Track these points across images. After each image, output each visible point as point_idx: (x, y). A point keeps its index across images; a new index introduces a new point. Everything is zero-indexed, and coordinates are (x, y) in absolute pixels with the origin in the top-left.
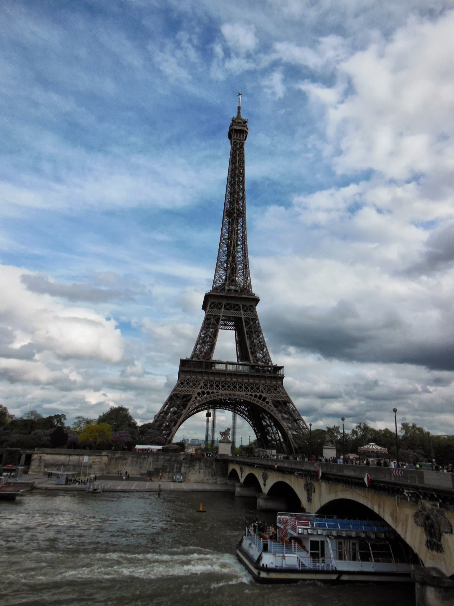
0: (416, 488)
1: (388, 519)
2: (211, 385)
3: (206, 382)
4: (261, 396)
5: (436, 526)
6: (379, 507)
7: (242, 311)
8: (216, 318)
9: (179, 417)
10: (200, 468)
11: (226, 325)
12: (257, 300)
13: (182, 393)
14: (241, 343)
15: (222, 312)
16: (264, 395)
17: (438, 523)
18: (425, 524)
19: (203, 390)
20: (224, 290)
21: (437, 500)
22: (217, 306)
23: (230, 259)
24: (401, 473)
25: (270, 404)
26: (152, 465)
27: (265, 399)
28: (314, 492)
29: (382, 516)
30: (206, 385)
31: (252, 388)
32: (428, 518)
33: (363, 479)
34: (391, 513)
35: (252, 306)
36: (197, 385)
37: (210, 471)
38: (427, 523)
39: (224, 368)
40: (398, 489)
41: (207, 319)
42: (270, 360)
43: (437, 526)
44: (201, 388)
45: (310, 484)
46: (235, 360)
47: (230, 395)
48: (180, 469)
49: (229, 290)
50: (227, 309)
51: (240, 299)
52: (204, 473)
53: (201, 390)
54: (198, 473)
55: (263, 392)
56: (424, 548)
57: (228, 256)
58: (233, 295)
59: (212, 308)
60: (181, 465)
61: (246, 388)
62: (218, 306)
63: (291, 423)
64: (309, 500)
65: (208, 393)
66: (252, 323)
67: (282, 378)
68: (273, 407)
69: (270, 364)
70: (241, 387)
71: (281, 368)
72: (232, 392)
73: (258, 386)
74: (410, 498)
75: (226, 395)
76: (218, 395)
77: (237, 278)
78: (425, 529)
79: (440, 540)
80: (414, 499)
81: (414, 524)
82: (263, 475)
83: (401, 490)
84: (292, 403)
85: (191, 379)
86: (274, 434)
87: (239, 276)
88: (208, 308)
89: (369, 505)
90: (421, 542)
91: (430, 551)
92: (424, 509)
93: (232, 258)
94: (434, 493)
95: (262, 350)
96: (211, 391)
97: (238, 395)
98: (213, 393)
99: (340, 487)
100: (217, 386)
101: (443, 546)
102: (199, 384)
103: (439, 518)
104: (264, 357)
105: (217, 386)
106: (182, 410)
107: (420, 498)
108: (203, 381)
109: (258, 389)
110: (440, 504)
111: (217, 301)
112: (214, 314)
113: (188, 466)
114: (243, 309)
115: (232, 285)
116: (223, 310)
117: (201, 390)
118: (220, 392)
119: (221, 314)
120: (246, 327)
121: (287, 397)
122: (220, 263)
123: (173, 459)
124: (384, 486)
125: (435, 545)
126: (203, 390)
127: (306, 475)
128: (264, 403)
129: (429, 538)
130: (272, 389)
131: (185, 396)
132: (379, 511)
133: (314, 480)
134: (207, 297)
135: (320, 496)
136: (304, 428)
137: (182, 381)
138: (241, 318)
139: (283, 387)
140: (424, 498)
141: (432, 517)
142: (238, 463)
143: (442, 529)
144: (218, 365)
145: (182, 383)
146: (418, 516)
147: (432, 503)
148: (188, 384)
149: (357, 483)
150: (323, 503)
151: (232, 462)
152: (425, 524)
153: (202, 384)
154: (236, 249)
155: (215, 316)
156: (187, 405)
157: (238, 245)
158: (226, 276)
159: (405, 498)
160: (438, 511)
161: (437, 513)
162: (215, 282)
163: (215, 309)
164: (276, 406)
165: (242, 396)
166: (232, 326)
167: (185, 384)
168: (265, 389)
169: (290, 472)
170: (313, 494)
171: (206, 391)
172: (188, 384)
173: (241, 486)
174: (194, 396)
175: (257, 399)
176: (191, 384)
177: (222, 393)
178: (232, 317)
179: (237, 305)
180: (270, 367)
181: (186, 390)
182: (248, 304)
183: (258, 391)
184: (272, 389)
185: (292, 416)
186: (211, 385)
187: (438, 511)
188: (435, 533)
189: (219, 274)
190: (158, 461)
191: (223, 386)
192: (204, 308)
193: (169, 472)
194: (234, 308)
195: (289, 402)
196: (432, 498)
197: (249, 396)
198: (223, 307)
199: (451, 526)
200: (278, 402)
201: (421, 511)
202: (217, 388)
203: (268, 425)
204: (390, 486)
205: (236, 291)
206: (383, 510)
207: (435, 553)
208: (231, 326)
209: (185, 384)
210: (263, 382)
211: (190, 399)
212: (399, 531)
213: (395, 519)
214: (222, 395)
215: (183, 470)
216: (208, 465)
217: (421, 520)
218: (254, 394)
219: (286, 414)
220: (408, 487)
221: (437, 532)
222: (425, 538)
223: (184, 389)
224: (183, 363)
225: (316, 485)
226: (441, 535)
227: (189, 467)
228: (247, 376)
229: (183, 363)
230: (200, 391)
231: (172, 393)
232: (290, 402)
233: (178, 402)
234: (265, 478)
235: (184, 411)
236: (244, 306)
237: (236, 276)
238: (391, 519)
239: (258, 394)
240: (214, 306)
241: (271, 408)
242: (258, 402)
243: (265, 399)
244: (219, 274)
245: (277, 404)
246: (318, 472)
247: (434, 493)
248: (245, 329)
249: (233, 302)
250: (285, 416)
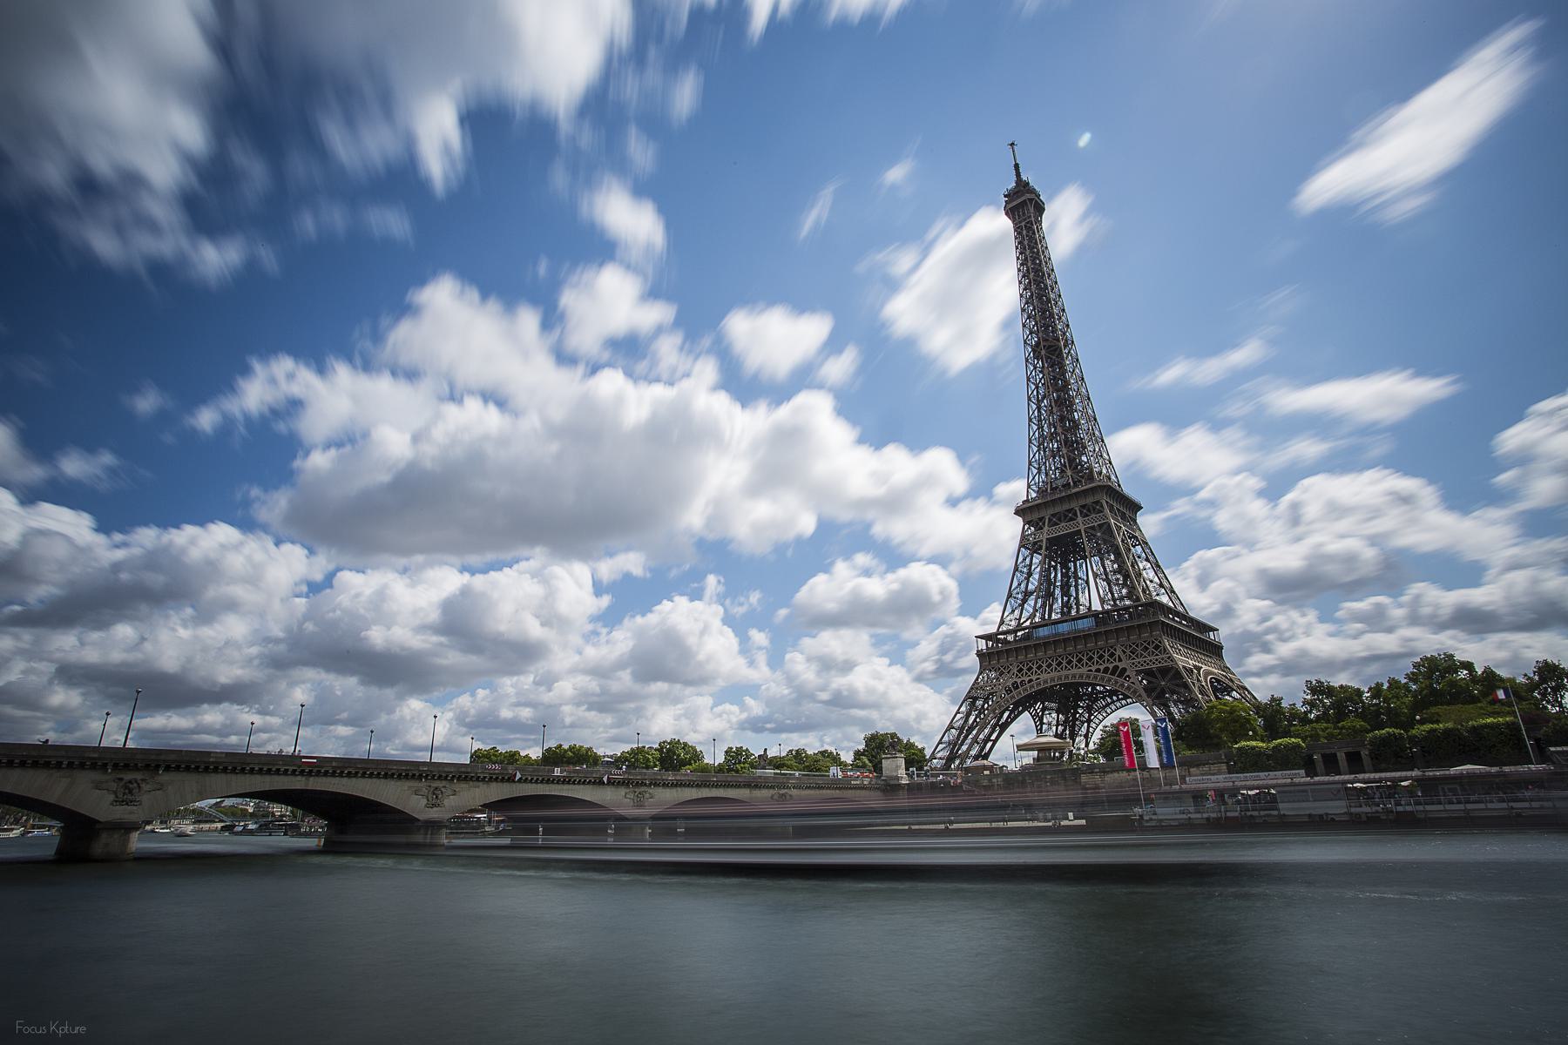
7: (1080, 519)
27: (1124, 670)
31: (1101, 657)
35: (1097, 503)
61: (1090, 659)
97: (1074, 676)
109: (1112, 655)
111: (1036, 516)
118: (1044, 676)
179: (1069, 511)
182: (1089, 500)
236: (1083, 507)
243: (1124, 670)
249: (1066, 507)
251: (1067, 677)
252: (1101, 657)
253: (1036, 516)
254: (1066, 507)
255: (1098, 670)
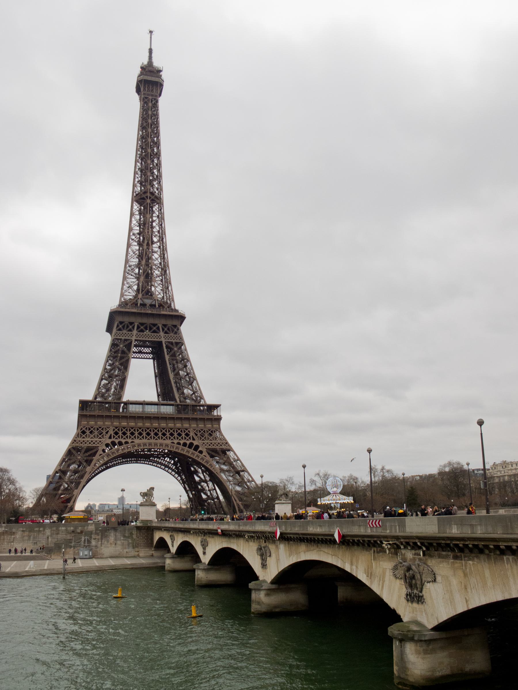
0: (397, 538)
1: (362, 577)
2: (124, 434)
3: (116, 430)
4: (191, 445)
5: (418, 576)
6: (352, 564)
7: (162, 334)
8: (127, 343)
9: (82, 477)
10: (116, 539)
11: (140, 352)
12: (181, 318)
13: (85, 446)
14: (162, 375)
15: (134, 336)
16: (195, 443)
17: (420, 573)
18: (405, 576)
19: (113, 440)
20: (137, 304)
21: (420, 548)
22: (128, 327)
23: (144, 262)
24: (379, 523)
25: (204, 454)
26: (50, 539)
27: (197, 447)
28: (270, 556)
29: (354, 574)
30: (116, 433)
31: (179, 435)
32: (409, 569)
33: (333, 535)
34: (365, 570)
35: (175, 326)
36: (104, 432)
37: (130, 541)
38: (407, 574)
39: (141, 410)
40: (375, 542)
41: (114, 345)
42: (202, 398)
43: (419, 577)
44: (110, 438)
45: (264, 547)
46: (154, 398)
47: (150, 444)
48: (89, 542)
49: (143, 305)
50: (142, 331)
51: (159, 316)
52: (123, 544)
53: (111, 440)
54: (114, 545)
55: (194, 439)
56: (403, 601)
57: (140, 257)
58: (150, 312)
59: (120, 330)
60: (91, 537)
61: (172, 434)
62: (128, 327)
63: (232, 476)
64: (264, 566)
65: (120, 444)
66: (176, 349)
67: (218, 419)
68: (208, 458)
69: (202, 402)
70: (164, 434)
71: (216, 407)
72: (153, 441)
73: (187, 431)
74: (389, 549)
75: (145, 444)
76: (134, 446)
77: (153, 289)
78: (406, 581)
79: (421, 592)
80: (393, 550)
81: (392, 578)
82: (201, 542)
83: (379, 542)
84: (233, 451)
85: (96, 427)
86: (209, 490)
87: (156, 285)
88: (114, 330)
89: (339, 565)
90: (399, 597)
91: (410, 604)
92: (405, 560)
93: (146, 261)
94: (417, 541)
95: (191, 384)
96: (123, 441)
97: (161, 445)
98: (126, 443)
99: (303, 547)
100: (132, 434)
101: (424, 597)
102: (107, 433)
103: (421, 568)
104: (194, 393)
105: (132, 434)
106: (85, 467)
107: (400, 548)
108: (112, 428)
109: (187, 435)
110: (424, 552)
111: (127, 320)
112: (123, 338)
113: (100, 537)
114: (163, 330)
115: (147, 298)
116: (135, 332)
117: (111, 440)
118: (137, 441)
119: (134, 338)
120: (168, 354)
121: (226, 443)
122: (128, 268)
123: (79, 531)
124: (358, 541)
125: (415, 597)
126: (113, 440)
127: (258, 538)
128: (197, 453)
129: (409, 590)
130: (206, 435)
131: (88, 449)
132: (351, 569)
133: (269, 542)
134: (113, 315)
135: (278, 560)
136: (249, 481)
137: (84, 429)
138: (161, 342)
139: (220, 432)
140: (405, 547)
141: (413, 567)
142: (167, 529)
143: (424, 579)
144: (131, 406)
145: (84, 432)
146: (397, 569)
147: (413, 552)
148: (91, 432)
149: (326, 541)
150: (281, 568)
151: (159, 529)
152: (405, 576)
153: (111, 432)
154: (150, 248)
155: (126, 340)
156: (91, 461)
157: (153, 242)
158: (138, 285)
159: (383, 551)
160: (420, 560)
161: (419, 563)
162: (122, 295)
163: (125, 331)
164: (212, 456)
165: (167, 445)
166: (149, 353)
167: (88, 432)
168: (196, 435)
169: (239, 535)
170: (268, 558)
171: (117, 441)
172: (91, 432)
173: (172, 558)
174: (100, 449)
175: (186, 448)
176: (96, 433)
177: (139, 443)
178: (149, 341)
179: (155, 325)
180: (203, 406)
181: (89, 441)
182: (170, 323)
183: (187, 438)
184: (206, 435)
185: (234, 467)
186: (124, 434)
187: (420, 560)
188: (416, 584)
189: (128, 283)
190: (58, 534)
191: (140, 434)
192: (109, 329)
193: (74, 547)
194: (151, 329)
195: (229, 450)
196: (415, 547)
197: (175, 445)
198: (136, 328)
199: (434, 574)
200: (215, 451)
201: (401, 563)
202: (133, 437)
203: (201, 480)
204: (366, 539)
205: (152, 306)
206: (357, 567)
207: (415, 605)
208: (147, 353)
209: (88, 432)
210: (194, 425)
211: (97, 451)
212: (375, 588)
213: (370, 574)
214: (139, 445)
215: (93, 543)
216: (127, 535)
217: (401, 572)
218: (182, 442)
219: (226, 465)
220: (386, 537)
221: (419, 583)
222: (404, 591)
223: (86, 439)
224: (84, 405)
225: (272, 547)
226: (422, 585)
227: (102, 539)
228: (172, 419)
229: (84, 405)
230: (109, 441)
231: (70, 445)
232: (230, 449)
233: (79, 457)
234: (204, 546)
235: (88, 469)
236: (165, 326)
237: (152, 285)
238: (365, 576)
239: (188, 442)
240: (123, 327)
241: (204, 458)
242: (188, 452)
243: (197, 447)
244: (128, 283)
245: (213, 453)
246: (276, 533)
247: (417, 541)
248: (167, 357)
249: (151, 321)
250: (225, 467)
251: (156, 444)
252: (179, 435)
253: (127, 320)
254: (151, 321)
255: (179, 444)
